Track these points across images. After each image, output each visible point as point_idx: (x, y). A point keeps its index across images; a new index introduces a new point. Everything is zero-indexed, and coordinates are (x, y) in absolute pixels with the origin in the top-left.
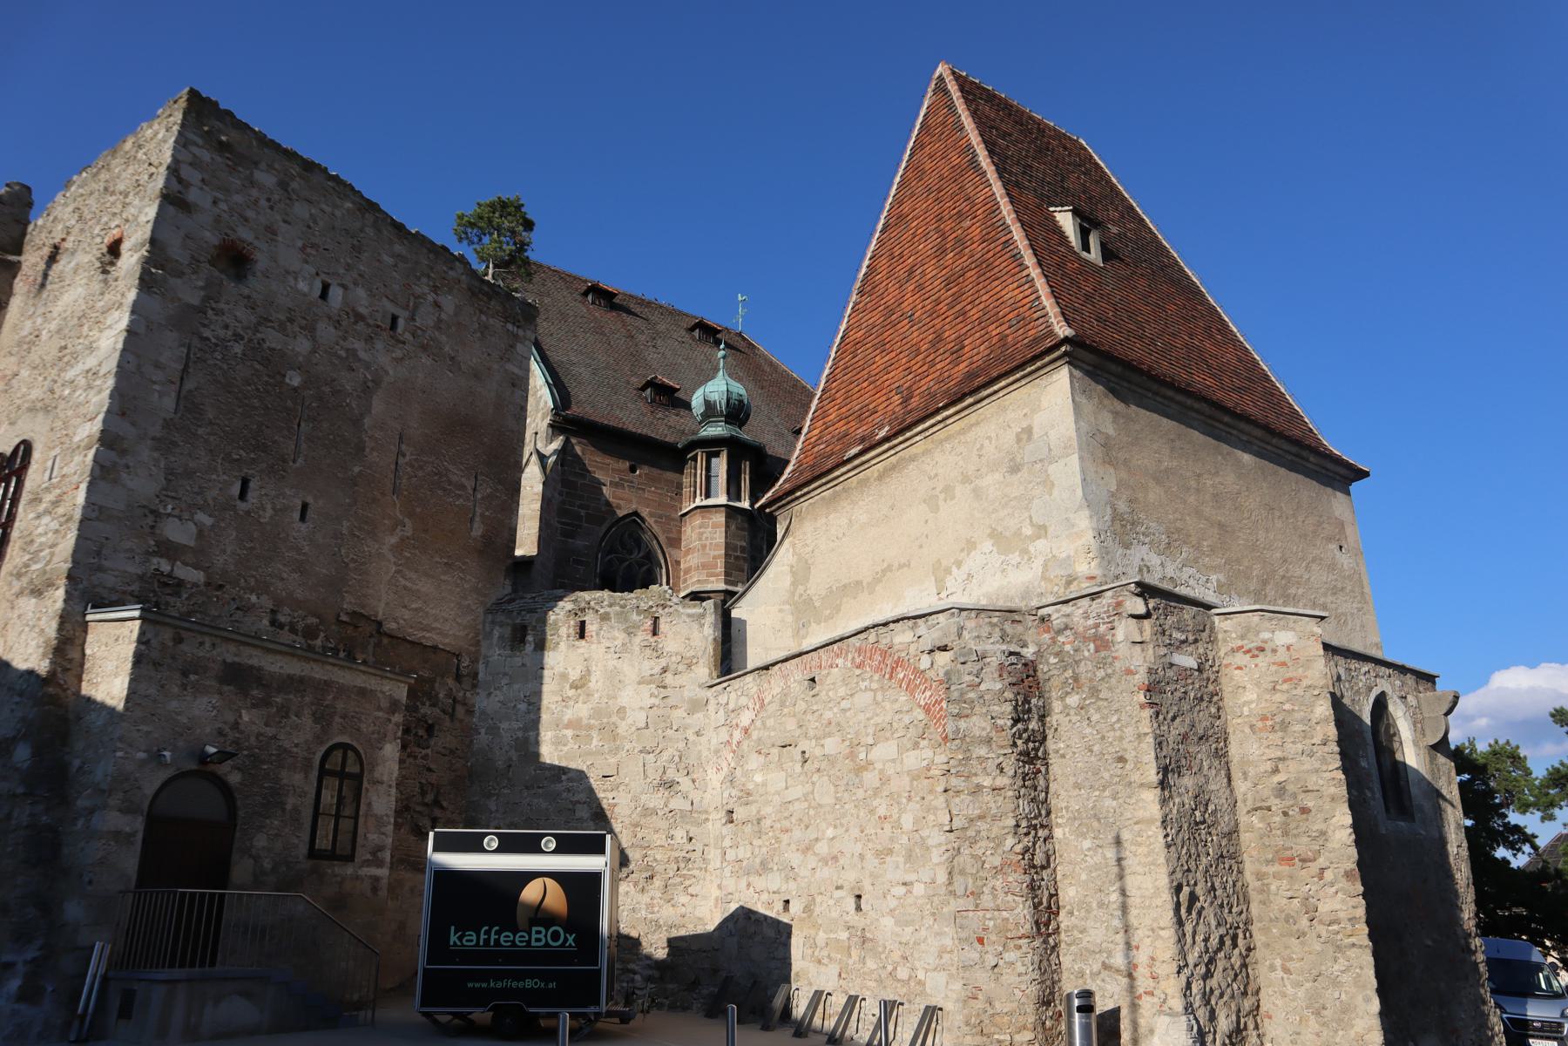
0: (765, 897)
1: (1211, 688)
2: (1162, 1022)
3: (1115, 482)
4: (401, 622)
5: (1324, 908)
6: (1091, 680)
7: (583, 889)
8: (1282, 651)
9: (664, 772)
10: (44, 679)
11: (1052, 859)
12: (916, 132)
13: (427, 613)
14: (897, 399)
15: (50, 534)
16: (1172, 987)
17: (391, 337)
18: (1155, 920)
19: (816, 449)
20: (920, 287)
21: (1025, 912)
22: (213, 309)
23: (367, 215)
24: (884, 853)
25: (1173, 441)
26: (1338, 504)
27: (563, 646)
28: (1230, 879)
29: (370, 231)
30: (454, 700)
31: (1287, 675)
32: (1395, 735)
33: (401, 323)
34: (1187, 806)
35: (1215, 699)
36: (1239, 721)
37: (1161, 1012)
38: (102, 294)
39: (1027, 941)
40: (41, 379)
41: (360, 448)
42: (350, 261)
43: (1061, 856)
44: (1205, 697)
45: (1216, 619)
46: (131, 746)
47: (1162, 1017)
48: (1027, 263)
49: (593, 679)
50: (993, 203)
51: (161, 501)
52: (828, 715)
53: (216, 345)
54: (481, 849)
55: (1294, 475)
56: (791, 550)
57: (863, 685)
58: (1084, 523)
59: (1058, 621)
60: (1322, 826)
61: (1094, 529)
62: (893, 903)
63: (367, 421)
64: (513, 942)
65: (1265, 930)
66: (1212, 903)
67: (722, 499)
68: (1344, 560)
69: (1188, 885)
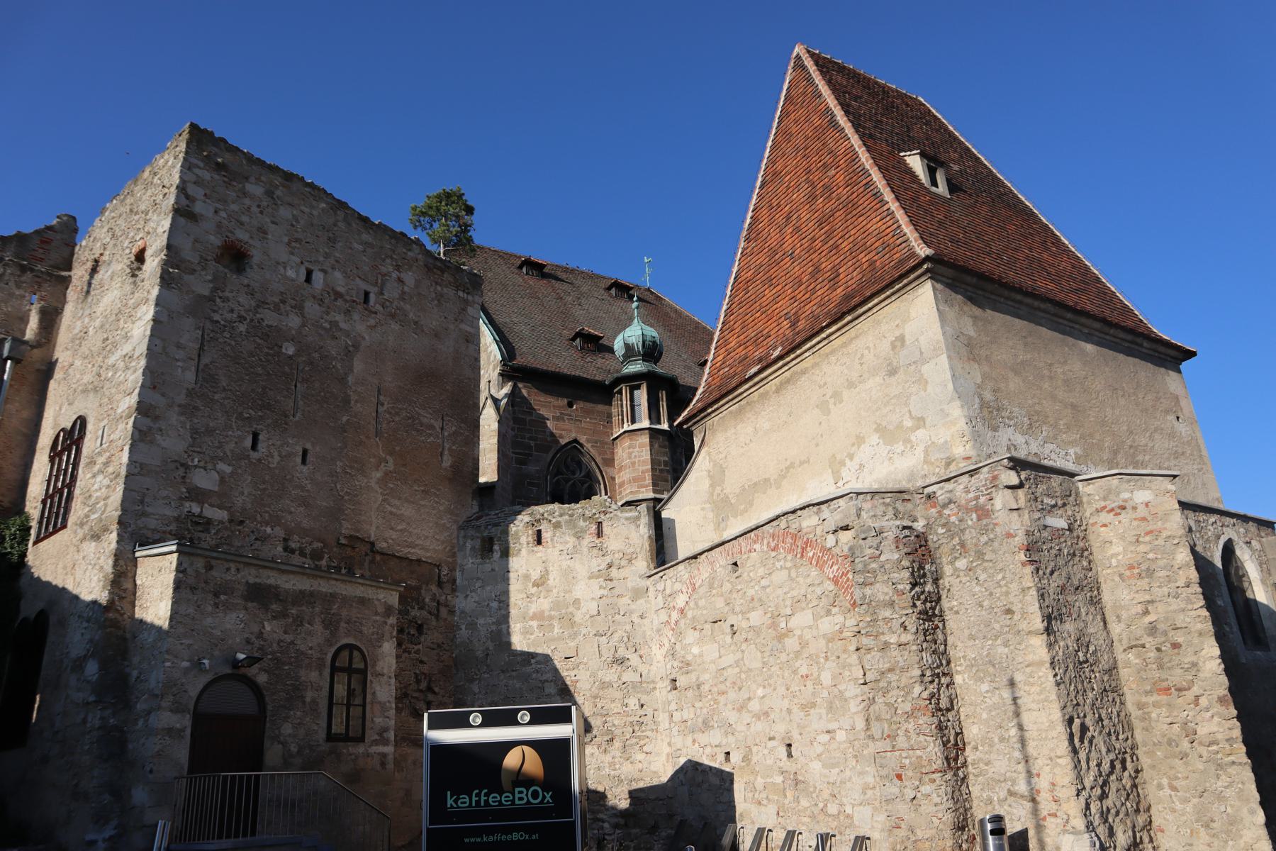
0: (708, 750)
1: (1081, 544)
2: (1067, 841)
3: (980, 376)
4: (390, 541)
5: (1203, 731)
6: (976, 545)
7: (555, 753)
8: (1141, 509)
9: (616, 651)
10: (105, 607)
11: (955, 702)
12: (781, 103)
13: (411, 533)
14: (786, 324)
15: (104, 490)
16: (1074, 808)
17: (366, 309)
18: (1052, 749)
19: (721, 372)
20: (797, 229)
21: (936, 749)
22: (220, 298)
23: (338, 212)
24: (808, 707)
25: (1025, 337)
26: (1171, 381)
27: (524, 552)
28: (1114, 710)
29: (342, 225)
30: (438, 603)
31: (1149, 529)
32: (1243, 576)
33: (372, 297)
34: (1071, 648)
35: (1086, 553)
36: (1109, 571)
37: (1065, 831)
38: (133, 293)
39: (940, 774)
40: (90, 366)
41: (346, 401)
42: (327, 251)
43: (963, 699)
44: (1077, 552)
45: (1080, 485)
46: (176, 657)
47: (1067, 835)
48: (886, 199)
49: (551, 577)
50: (852, 153)
51: (189, 456)
52: (751, 592)
53: (225, 326)
54: (468, 725)
55: (1130, 359)
56: (707, 458)
57: (778, 565)
58: (957, 412)
59: (943, 497)
60: (1194, 659)
61: (965, 417)
62: (819, 749)
63: (351, 379)
64: (500, 801)
65: (1150, 754)
66: (1101, 732)
67: (645, 423)
68: (1182, 428)
69: (1078, 717)
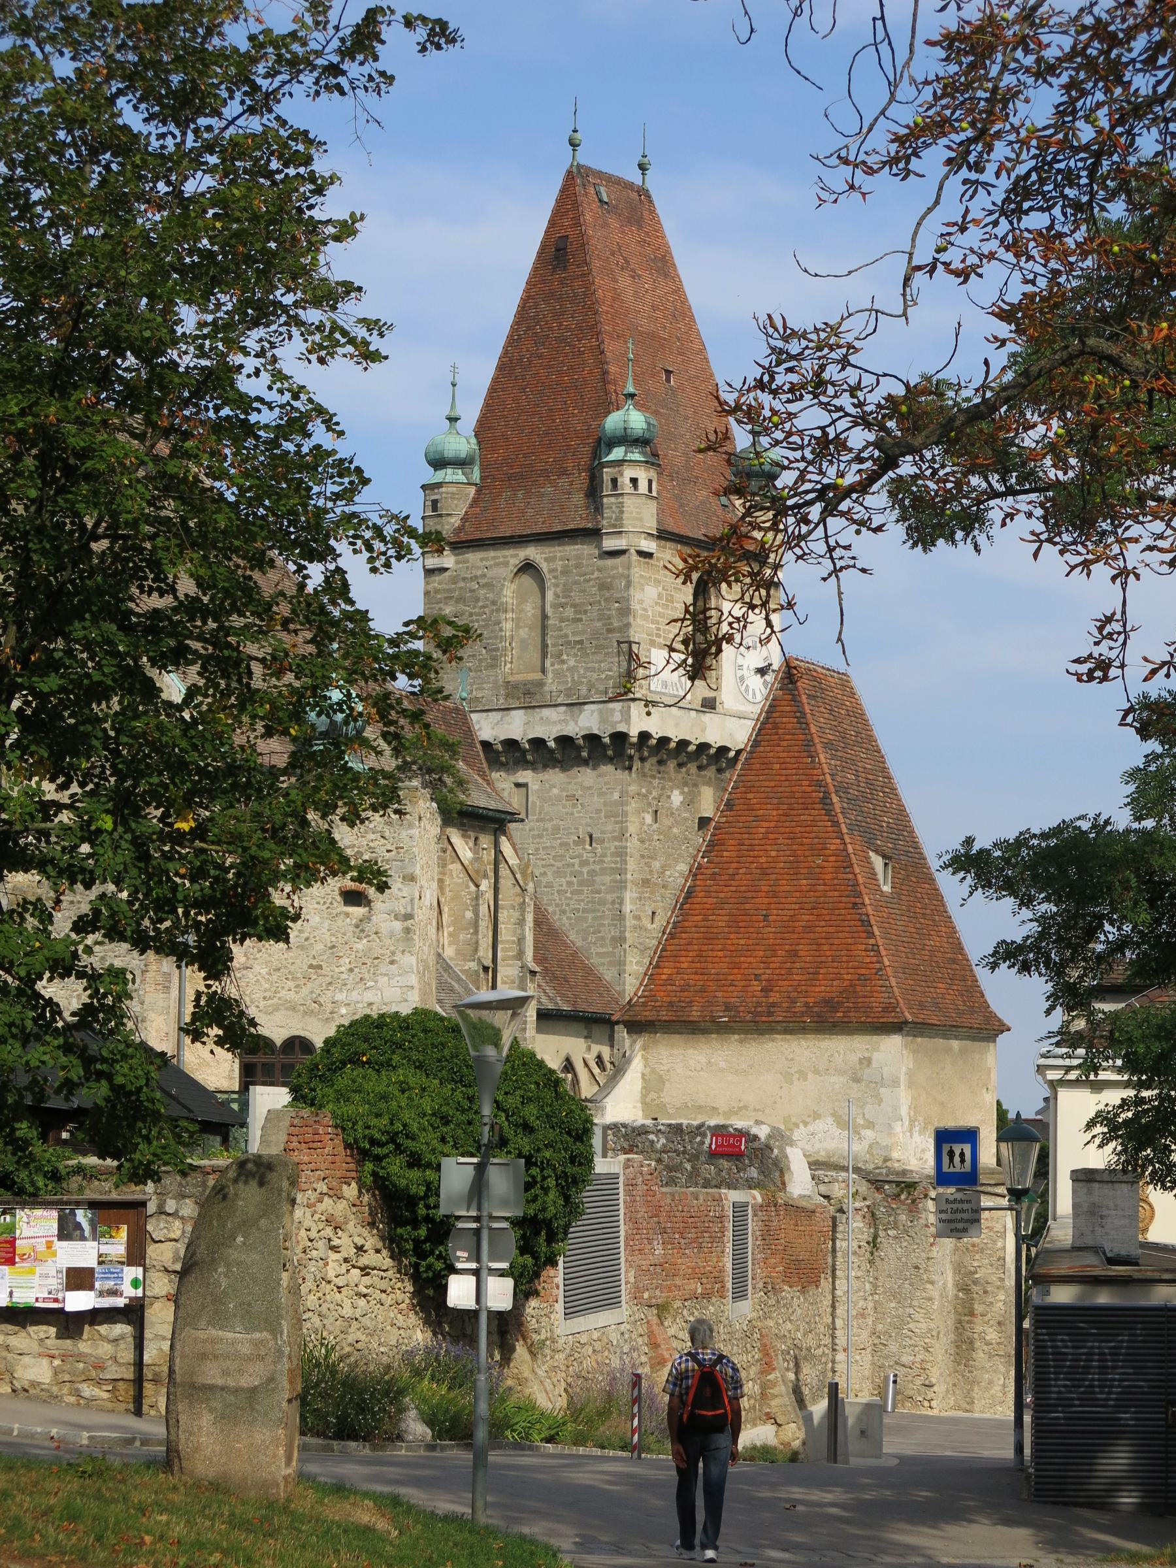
14: (756, 986)
